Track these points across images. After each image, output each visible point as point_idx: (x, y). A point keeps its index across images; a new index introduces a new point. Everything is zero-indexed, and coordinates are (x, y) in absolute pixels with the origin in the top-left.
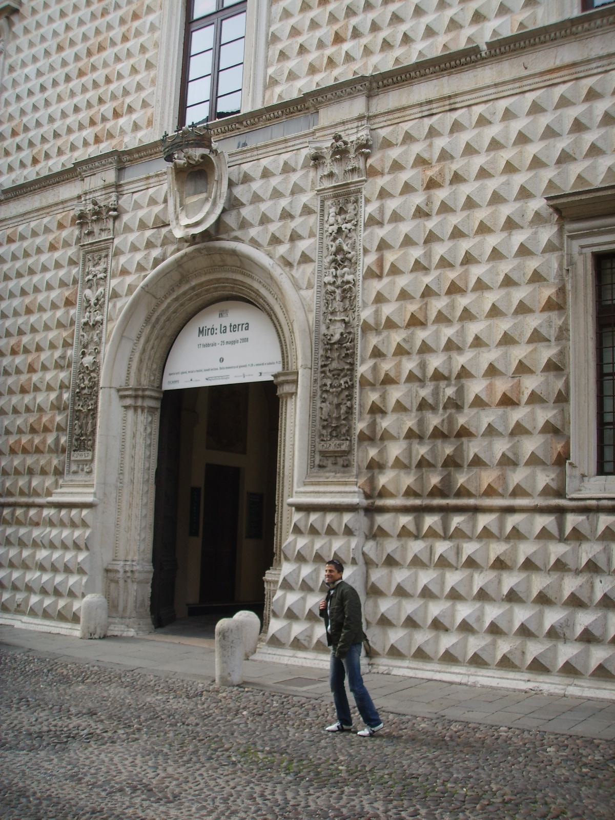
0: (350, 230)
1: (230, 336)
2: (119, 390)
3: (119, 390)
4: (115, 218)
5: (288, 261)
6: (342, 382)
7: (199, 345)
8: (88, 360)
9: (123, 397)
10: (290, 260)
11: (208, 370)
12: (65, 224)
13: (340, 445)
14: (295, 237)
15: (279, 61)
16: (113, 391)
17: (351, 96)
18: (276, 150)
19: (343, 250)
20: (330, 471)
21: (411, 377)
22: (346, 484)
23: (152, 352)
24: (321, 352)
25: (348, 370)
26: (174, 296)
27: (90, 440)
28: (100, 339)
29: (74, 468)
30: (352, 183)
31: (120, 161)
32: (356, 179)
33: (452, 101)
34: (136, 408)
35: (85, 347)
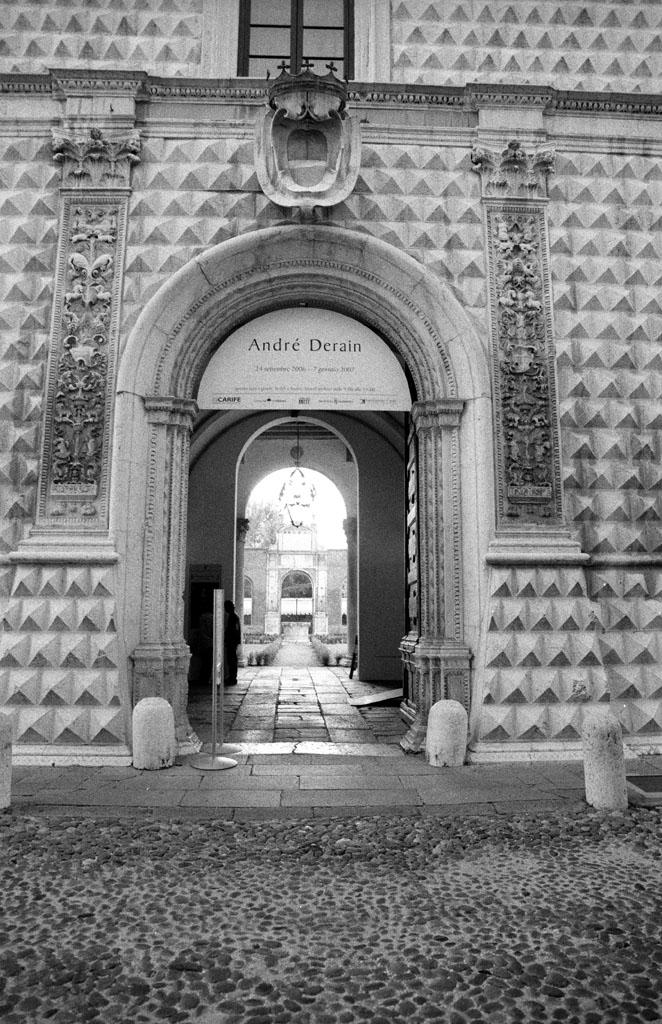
0: (529, 251)
2: (143, 400)
3: (143, 400)
4: (134, 165)
5: (447, 269)
6: (536, 419)
8: (81, 352)
9: (148, 410)
10: (451, 270)
12: (22, 154)
13: (540, 492)
14: (452, 244)
15: (410, 40)
16: (137, 400)
17: (527, 105)
19: (522, 272)
20: (526, 521)
21: (626, 422)
22: (555, 536)
23: (194, 355)
24: (500, 381)
25: (542, 406)
26: (241, 285)
27: (92, 467)
28: (107, 324)
29: (56, 507)
30: (531, 200)
31: (143, 90)
32: (535, 197)
33: (647, 146)
34: (170, 427)
35: (74, 332)
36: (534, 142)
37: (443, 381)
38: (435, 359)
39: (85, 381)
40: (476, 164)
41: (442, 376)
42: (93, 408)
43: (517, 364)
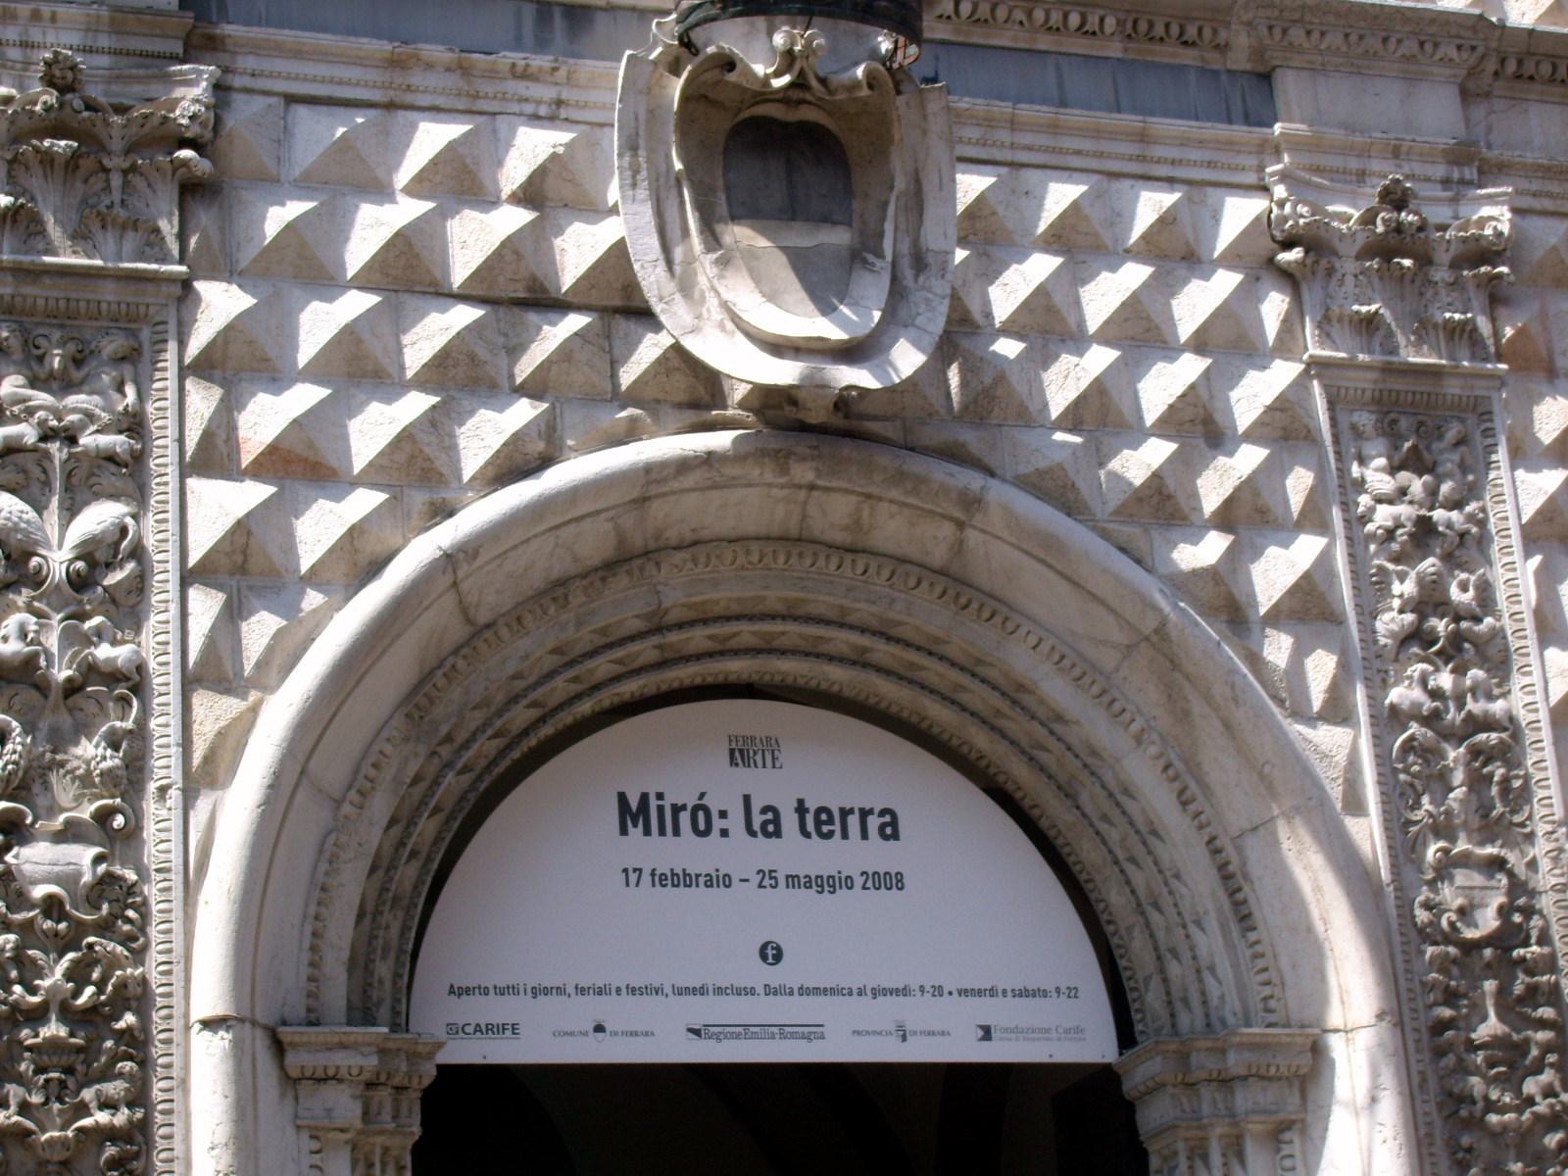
0: (1463, 535)
1: (794, 852)
7: (631, 875)
11: (702, 991)
18: (1100, 155)
36: (1446, 183)
37: (1235, 966)
38: (1201, 886)
39: (69, 976)
40: (1287, 245)
41: (1230, 945)
42: (106, 1075)
43: (1462, 912)
